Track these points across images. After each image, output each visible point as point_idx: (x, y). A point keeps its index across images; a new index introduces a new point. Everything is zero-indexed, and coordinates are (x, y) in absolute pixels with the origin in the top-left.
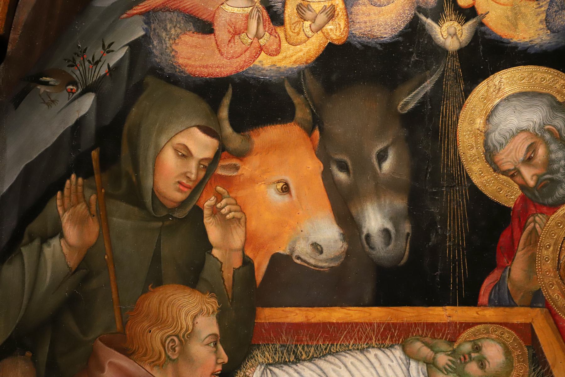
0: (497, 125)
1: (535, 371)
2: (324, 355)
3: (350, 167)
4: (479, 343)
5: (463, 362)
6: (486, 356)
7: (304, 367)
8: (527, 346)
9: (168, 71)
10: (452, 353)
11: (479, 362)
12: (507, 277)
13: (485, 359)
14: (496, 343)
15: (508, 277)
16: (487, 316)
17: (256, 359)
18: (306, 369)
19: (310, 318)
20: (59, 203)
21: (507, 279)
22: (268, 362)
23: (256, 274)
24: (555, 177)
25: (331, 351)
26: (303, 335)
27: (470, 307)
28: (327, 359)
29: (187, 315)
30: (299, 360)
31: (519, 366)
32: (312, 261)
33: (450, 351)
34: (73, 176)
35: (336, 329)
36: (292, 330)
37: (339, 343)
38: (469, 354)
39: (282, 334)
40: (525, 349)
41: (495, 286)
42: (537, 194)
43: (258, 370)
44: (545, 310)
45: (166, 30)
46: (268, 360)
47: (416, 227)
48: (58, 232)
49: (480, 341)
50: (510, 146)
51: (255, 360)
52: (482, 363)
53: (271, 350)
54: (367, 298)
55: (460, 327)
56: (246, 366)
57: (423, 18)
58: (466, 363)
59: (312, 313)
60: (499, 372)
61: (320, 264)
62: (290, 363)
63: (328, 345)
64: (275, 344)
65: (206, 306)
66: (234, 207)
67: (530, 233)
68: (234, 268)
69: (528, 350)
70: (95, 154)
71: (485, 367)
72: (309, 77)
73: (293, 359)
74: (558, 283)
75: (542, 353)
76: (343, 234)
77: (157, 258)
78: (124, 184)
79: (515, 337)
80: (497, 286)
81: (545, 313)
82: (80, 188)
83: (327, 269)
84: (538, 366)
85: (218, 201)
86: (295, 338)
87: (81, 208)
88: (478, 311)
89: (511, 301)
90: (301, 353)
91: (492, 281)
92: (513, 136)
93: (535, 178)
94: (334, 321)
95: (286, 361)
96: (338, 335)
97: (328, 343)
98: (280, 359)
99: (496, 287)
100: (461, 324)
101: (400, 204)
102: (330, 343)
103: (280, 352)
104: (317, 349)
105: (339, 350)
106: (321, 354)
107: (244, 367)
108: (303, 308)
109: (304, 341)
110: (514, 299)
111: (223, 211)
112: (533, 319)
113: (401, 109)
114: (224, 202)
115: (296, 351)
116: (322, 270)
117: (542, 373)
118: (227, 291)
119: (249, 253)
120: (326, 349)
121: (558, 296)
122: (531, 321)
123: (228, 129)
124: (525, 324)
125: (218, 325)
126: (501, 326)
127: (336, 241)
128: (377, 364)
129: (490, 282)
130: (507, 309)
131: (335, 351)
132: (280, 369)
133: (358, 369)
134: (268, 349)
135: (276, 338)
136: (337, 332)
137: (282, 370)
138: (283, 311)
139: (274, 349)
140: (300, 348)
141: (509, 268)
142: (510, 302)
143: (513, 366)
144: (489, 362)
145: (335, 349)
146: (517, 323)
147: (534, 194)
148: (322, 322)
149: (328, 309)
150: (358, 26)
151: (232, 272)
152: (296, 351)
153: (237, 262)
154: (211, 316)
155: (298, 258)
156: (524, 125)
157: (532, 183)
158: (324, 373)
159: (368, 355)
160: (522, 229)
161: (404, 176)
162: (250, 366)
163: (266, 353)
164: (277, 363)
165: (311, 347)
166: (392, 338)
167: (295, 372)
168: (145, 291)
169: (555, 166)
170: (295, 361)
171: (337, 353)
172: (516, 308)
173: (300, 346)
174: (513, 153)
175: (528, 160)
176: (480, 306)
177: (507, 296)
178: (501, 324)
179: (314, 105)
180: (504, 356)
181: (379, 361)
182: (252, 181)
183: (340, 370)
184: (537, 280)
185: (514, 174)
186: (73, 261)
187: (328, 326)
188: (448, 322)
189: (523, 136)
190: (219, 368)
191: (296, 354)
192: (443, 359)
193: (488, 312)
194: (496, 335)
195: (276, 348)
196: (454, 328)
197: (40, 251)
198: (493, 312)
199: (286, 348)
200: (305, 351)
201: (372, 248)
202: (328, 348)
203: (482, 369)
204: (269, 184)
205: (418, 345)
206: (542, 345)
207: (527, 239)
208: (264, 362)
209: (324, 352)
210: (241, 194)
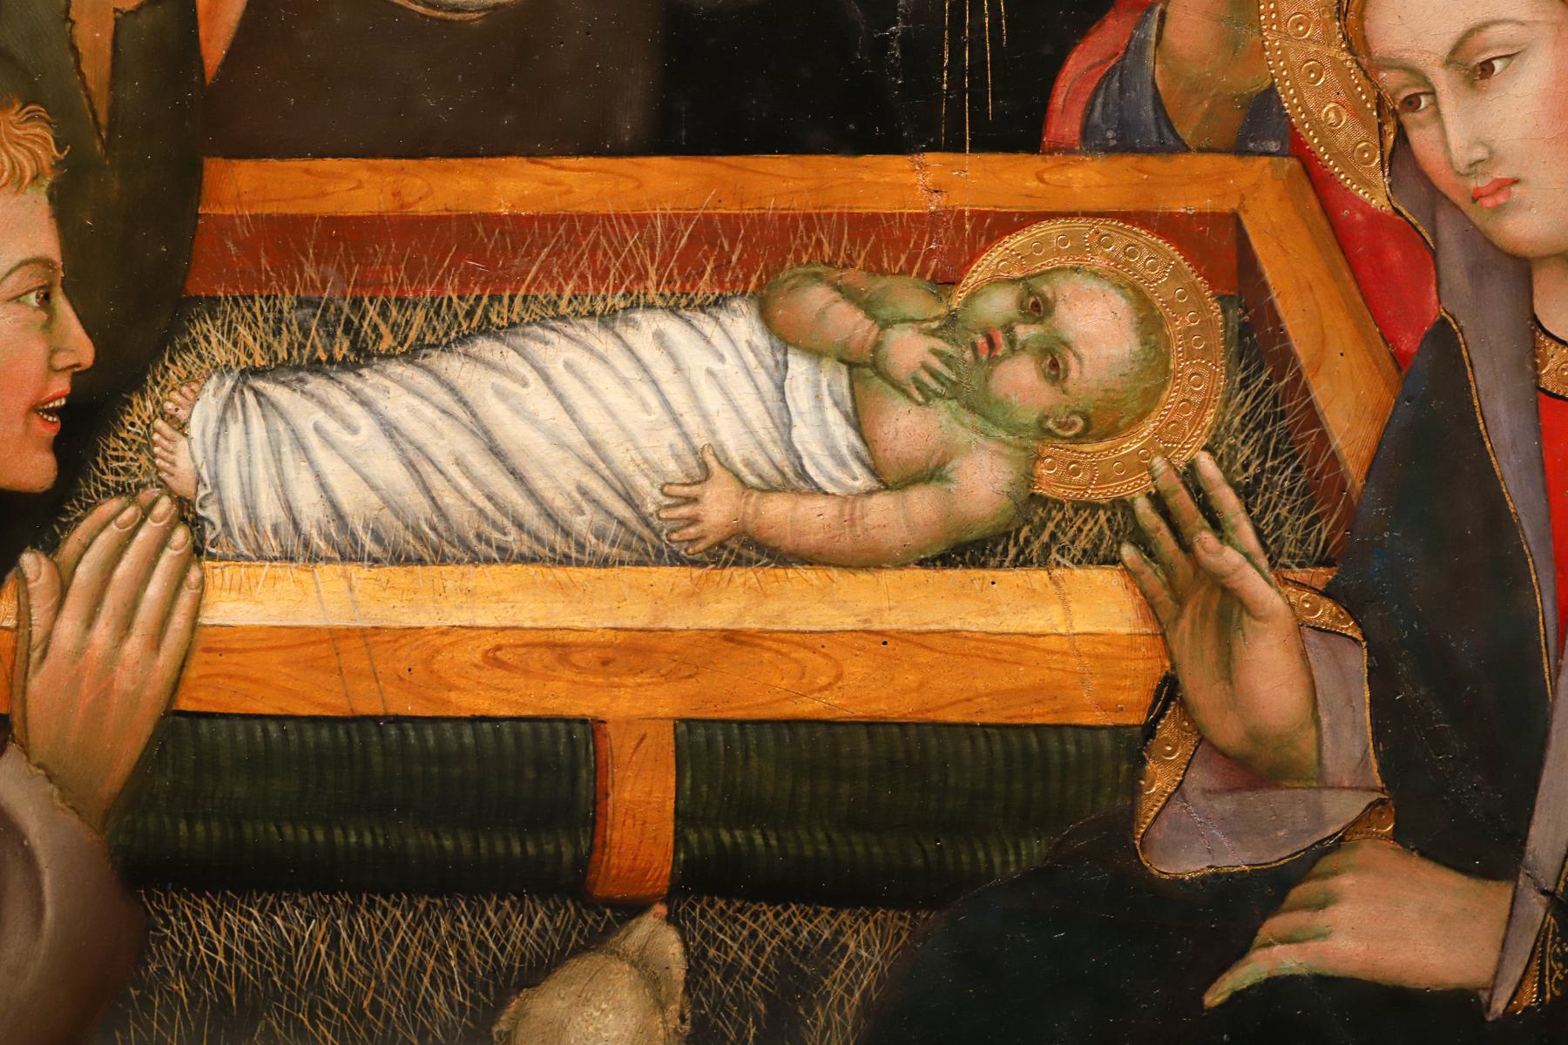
1: (1248, 386)
2: (464, 335)
4: (1045, 288)
5: (984, 357)
6: (1069, 335)
7: (387, 383)
8: (1220, 299)
10: (945, 326)
11: (1045, 357)
12: (1153, 45)
13: (1066, 344)
14: (1106, 287)
15: (1157, 44)
16: (1077, 187)
17: (204, 352)
19: (410, 199)
21: (1150, 52)
22: (250, 362)
23: (202, 33)
25: (489, 320)
26: (384, 263)
27: (1013, 156)
28: (475, 349)
30: (369, 356)
31: (1190, 371)
33: (936, 318)
35: (508, 240)
36: (342, 244)
37: (522, 292)
38: (1008, 328)
39: (302, 259)
40: (1215, 308)
41: (1108, 76)
43: (211, 392)
44: (1290, 163)
46: (250, 356)
49: (1047, 282)
51: (200, 356)
52: (1053, 362)
53: (260, 319)
54: (627, 127)
55: (974, 229)
56: (162, 377)
58: (994, 360)
59: (419, 182)
60: (1114, 390)
62: (335, 368)
63: (479, 298)
64: (276, 297)
65: (7, 152)
68: (116, 10)
69: (1224, 311)
71: (1066, 376)
73: (345, 351)
74: (1337, 65)
75: (1277, 320)
79: (1178, 263)
80: (1116, 77)
81: (1290, 175)
83: (477, 15)
84: (1260, 369)
86: (351, 272)
88: (1044, 171)
89: (1165, 130)
90: (375, 328)
91: (1098, 60)
94: (504, 211)
95: (319, 361)
96: (516, 262)
97: (477, 292)
98: (295, 353)
99: (1110, 80)
100: (979, 217)
102: (488, 292)
103: (295, 328)
104: (437, 313)
105: (522, 319)
106: (453, 334)
107: (157, 383)
108: (386, 162)
109: (387, 285)
110: (1175, 125)
112: (1243, 198)
115: (356, 322)
116: (457, 17)
117: (1271, 395)
118: (89, 97)
120: (470, 314)
121: (1338, 114)
122: (1235, 205)
124: (1214, 214)
125: (54, 226)
126: (1125, 223)
128: (662, 369)
129: (1089, 63)
130: (1152, 163)
131: (506, 324)
132: (294, 390)
133: (591, 389)
134: (248, 315)
135: (279, 275)
136: (515, 250)
137: (303, 392)
138: (307, 171)
139: (271, 316)
140: (372, 312)
141: (1158, 8)
142: (1160, 135)
143: (1167, 371)
144: (1079, 358)
145: (505, 311)
146: (1185, 214)
148: (455, 213)
149: (480, 165)
151: (112, 24)
152: (356, 322)
154: (28, 190)
158: (464, 403)
159: (630, 335)
162: (179, 378)
163: (241, 329)
164: (282, 365)
165: (415, 308)
166: (719, 270)
167: (352, 399)
170: (352, 358)
171: (513, 330)
172: (1182, 159)
173: (371, 302)
176: (1051, 152)
177: (1151, 114)
178: (1125, 217)
180: (1134, 335)
181: (672, 356)
183: (524, 391)
184: (1262, 55)
187: (480, 229)
188: (932, 213)
190: (62, 385)
191: (357, 333)
193: (1080, 175)
194: (1108, 256)
195: (281, 312)
196: (951, 232)
198: (1098, 172)
199: (319, 312)
200: (391, 321)
202: (479, 312)
203: (1053, 385)
205: (817, 297)
206: (1274, 294)
208: (233, 363)
209: (465, 326)
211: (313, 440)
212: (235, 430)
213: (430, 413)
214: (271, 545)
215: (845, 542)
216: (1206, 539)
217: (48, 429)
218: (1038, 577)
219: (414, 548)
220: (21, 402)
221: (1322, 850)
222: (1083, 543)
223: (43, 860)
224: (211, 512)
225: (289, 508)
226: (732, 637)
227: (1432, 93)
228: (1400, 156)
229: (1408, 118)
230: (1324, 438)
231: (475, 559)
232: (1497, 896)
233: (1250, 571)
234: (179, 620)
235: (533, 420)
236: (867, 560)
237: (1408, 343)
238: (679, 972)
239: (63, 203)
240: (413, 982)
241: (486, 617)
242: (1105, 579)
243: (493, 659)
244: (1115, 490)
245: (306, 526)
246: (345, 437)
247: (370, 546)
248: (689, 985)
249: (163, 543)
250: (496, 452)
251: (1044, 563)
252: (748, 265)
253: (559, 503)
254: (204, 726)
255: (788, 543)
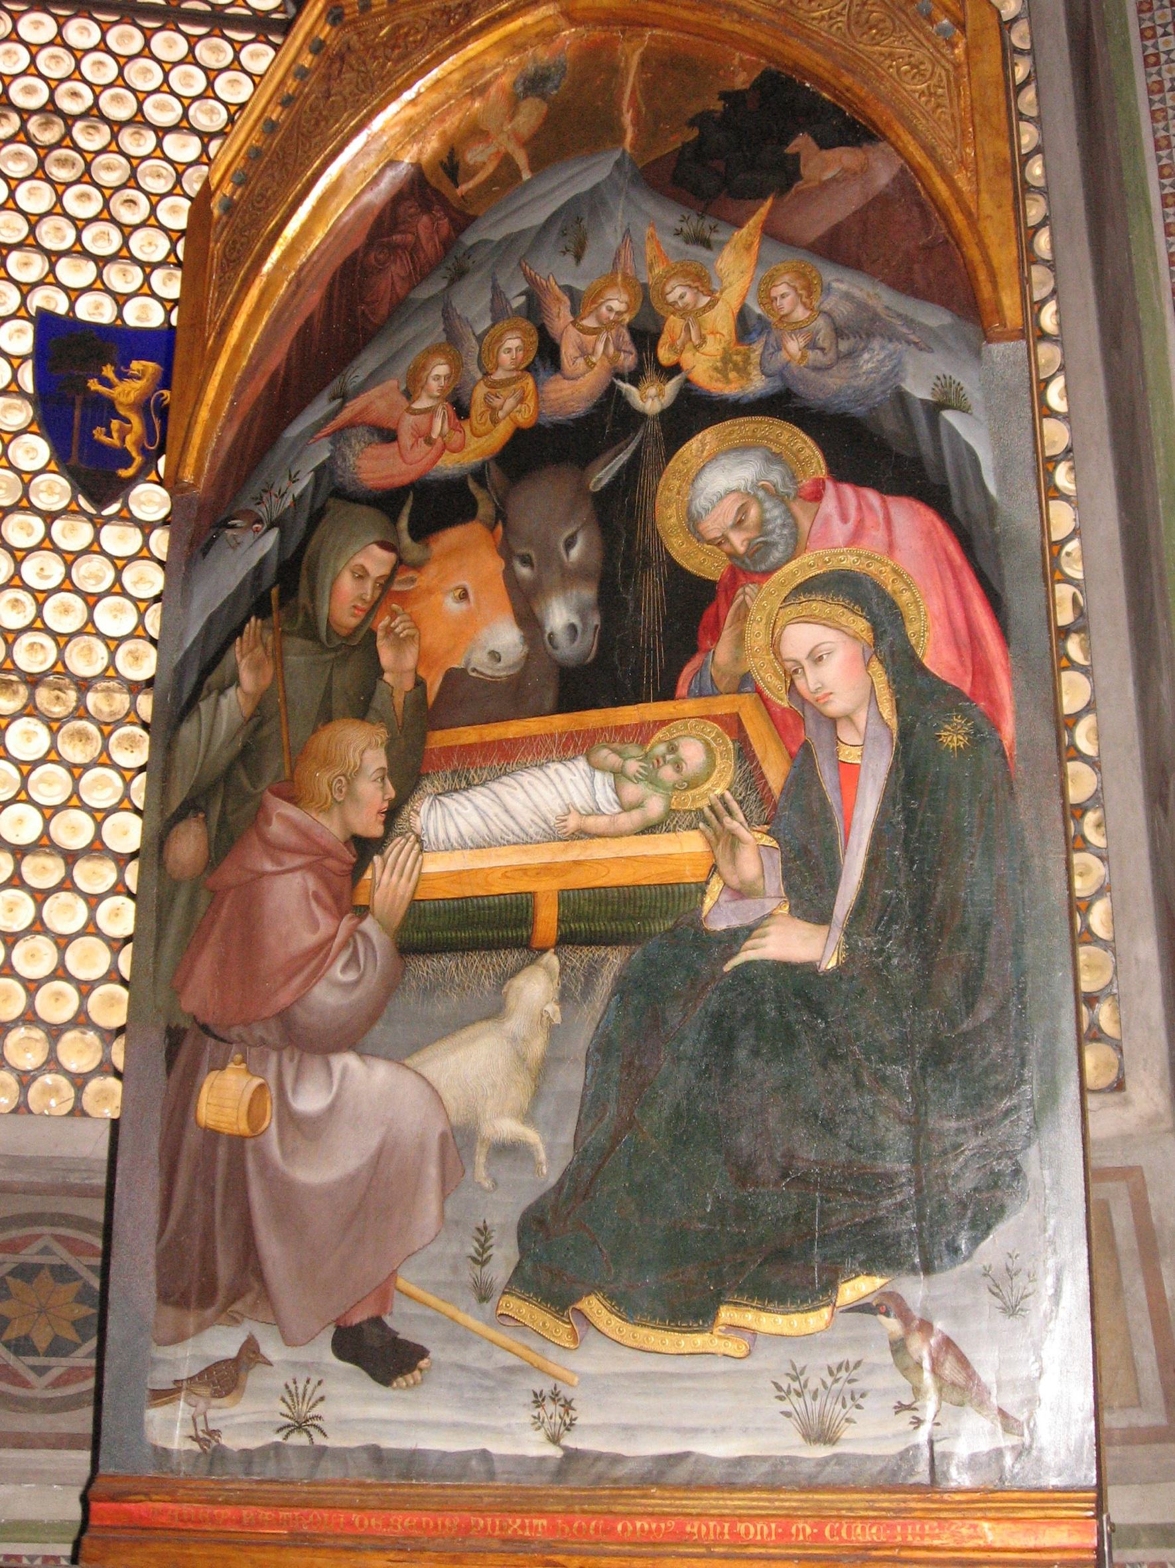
0: (703, 489)
3: (535, 561)
9: (351, 489)
18: (479, 795)
20: (237, 649)
24: (768, 539)
29: (355, 751)
32: (489, 672)
34: (253, 619)
42: (747, 561)
44: (755, 695)
45: (350, 446)
47: (606, 620)
48: (235, 680)
50: (718, 510)
52: (678, 766)
57: (620, 383)
61: (497, 674)
66: (408, 624)
67: (739, 607)
70: (274, 592)
72: (493, 466)
76: (524, 637)
77: (328, 694)
78: (301, 618)
82: (258, 631)
85: (393, 619)
87: (259, 651)
92: (721, 499)
93: (745, 543)
101: (588, 593)
111: (397, 630)
113: (595, 485)
114: (397, 621)
119: (421, 673)
123: (406, 540)
127: (516, 646)
128: (556, 780)
130: (710, 699)
133: (535, 789)
140: (472, 772)
147: (743, 562)
150: (548, 404)
153: (409, 684)
155: (474, 670)
156: (734, 485)
157: (741, 549)
160: (729, 603)
161: (595, 559)
168: (315, 731)
169: (770, 527)
172: (720, 698)
174: (720, 519)
175: (738, 524)
178: (702, 717)
179: (498, 499)
181: (560, 776)
182: (430, 591)
185: (721, 542)
186: (248, 709)
189: (733, 497)
190: (386, 805)
192: (633, 766)
197: (218, 701)
201: (556, 648)
204: (446, 593)
207: (735, 614)
210: (415, 608)
211: (454, 813)
212: (433, 812)
213: (487, 801)
214: (442, 847)
215: (612, 830)
216: (727, 819)
217: (382, 818)
218: (672, 835)
219: (483, 844)
220: (375, 812)
221: (764, 918)
222: (687, 823)
223: (377, 949)
224: (425, 838)
225: (447, 834)
226: (575, 862)
227: (803, 668)
228: (792, 689)
229: (795, 676)
230: (766, 783)
231: (500, 845)
232: (824, 930)
233: (742, 829)
234: (416, 872)
235: (518, 800)
236: (618, 835)
237: (795, 749)
238: (557, 970)
239: (388, 750)
240: (479, 979)
241: (502, 864)
242: (694, 834)
243: (505, 876)
244: (699, 805)
245: (452, 840)
246: (463, 811)
247: (470, 844)
248: (560, 974)
249: (412, 849)
250: (507, 811)
251: (674, 831)
252: (583, 745)
253: (525, 825)
254: (422, 904)
255: (594, 831)
